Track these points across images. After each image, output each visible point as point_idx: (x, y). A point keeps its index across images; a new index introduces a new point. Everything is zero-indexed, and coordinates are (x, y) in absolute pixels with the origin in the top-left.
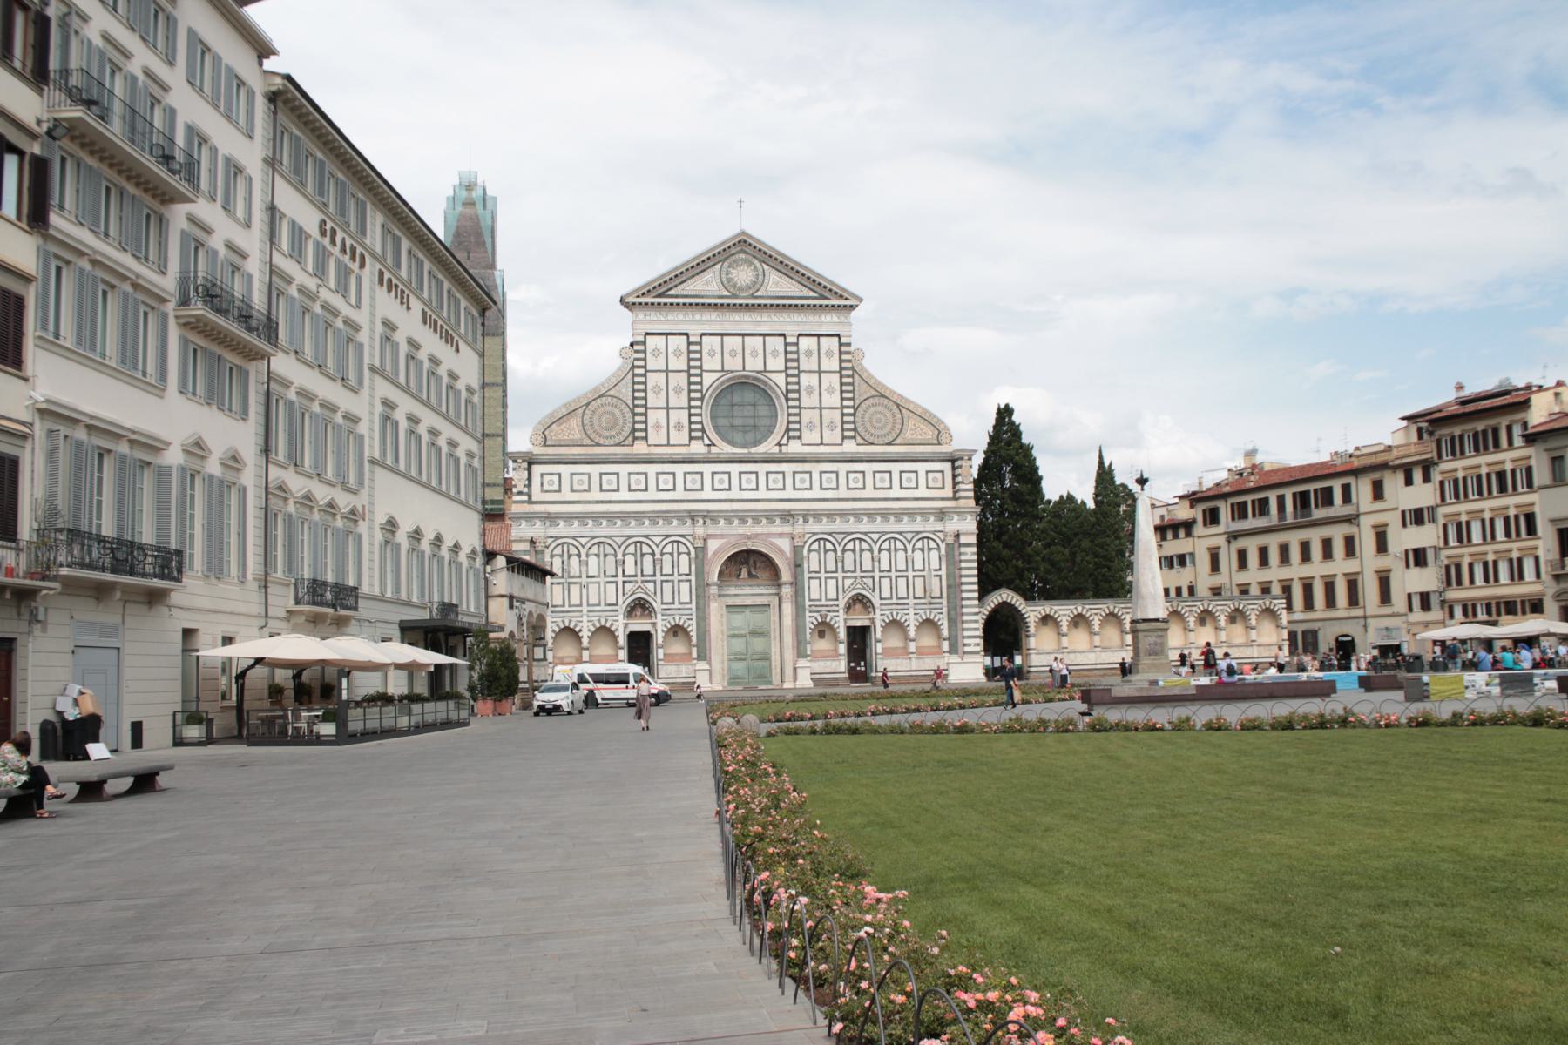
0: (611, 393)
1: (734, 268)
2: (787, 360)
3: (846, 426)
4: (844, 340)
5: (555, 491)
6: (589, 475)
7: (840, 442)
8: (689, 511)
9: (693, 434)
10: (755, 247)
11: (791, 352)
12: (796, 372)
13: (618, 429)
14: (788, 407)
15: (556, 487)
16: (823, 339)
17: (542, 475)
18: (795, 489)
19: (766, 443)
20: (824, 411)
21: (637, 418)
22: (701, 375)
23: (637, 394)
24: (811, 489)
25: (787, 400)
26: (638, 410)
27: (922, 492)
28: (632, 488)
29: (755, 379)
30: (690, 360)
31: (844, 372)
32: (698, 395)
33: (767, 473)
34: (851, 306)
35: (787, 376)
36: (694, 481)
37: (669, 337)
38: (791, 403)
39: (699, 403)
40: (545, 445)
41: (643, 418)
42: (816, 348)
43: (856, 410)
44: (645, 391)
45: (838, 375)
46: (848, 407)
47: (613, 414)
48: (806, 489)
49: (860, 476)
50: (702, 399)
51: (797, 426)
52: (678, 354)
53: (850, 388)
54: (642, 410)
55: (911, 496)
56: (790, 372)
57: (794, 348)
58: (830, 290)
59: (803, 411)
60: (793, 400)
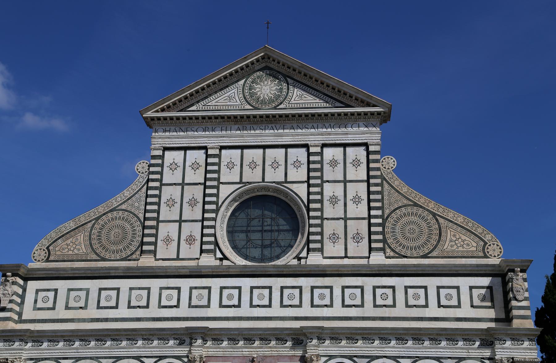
0: (123, 207)
1: (257, 84)
2: (309, 170)
3: (373, 237)
4: (372, 148)
5: (49, 309)
6: (88, 291)
7: (368, 255)
8: (187, 328)
9: (204, 247)
10: (279, 63)
11: (314, 162)
12: (319, 181)
13: (125, 244)
14: (309, 218)
15: (50, 304)
16: (349, 150)
17: (37, 291)
18: (312, 306)
19: (285, 258)
20: (349, 222)
21: (147, 231)
22: (217, 188)
23: (149, 207)
24: (331, 306)
25: (308, 210)
26: (148, 223)
27: (466, 311)
28: (132, 305)
29: (277, 190)
30: (207, 172)
31: (372, 181)
32: (213, 207)
33: (282, 288)
34: (379, 113)
35: (309, 186)
36: (200, 297)
37: (188, 152)
38: (312, 214)
39: (213, 215)
40: (48, 260)
41: (153, 231)
42: (342, 158)
43: (385, 221)
44: (159, 204)
45: (365, 184)
46: (376, 217)
47: (123, 228)
48: (326, 306)
49: (389, 292)
50: (216, 211)
51: (318, 238)
52: (195, 166)
53: (379, 197)
54: (153, 223)
55: (452, 316)
56: (312, 182)
57: (317, 158)
58: (356, 99)
59: (325, 222)
60: (315, 210)
